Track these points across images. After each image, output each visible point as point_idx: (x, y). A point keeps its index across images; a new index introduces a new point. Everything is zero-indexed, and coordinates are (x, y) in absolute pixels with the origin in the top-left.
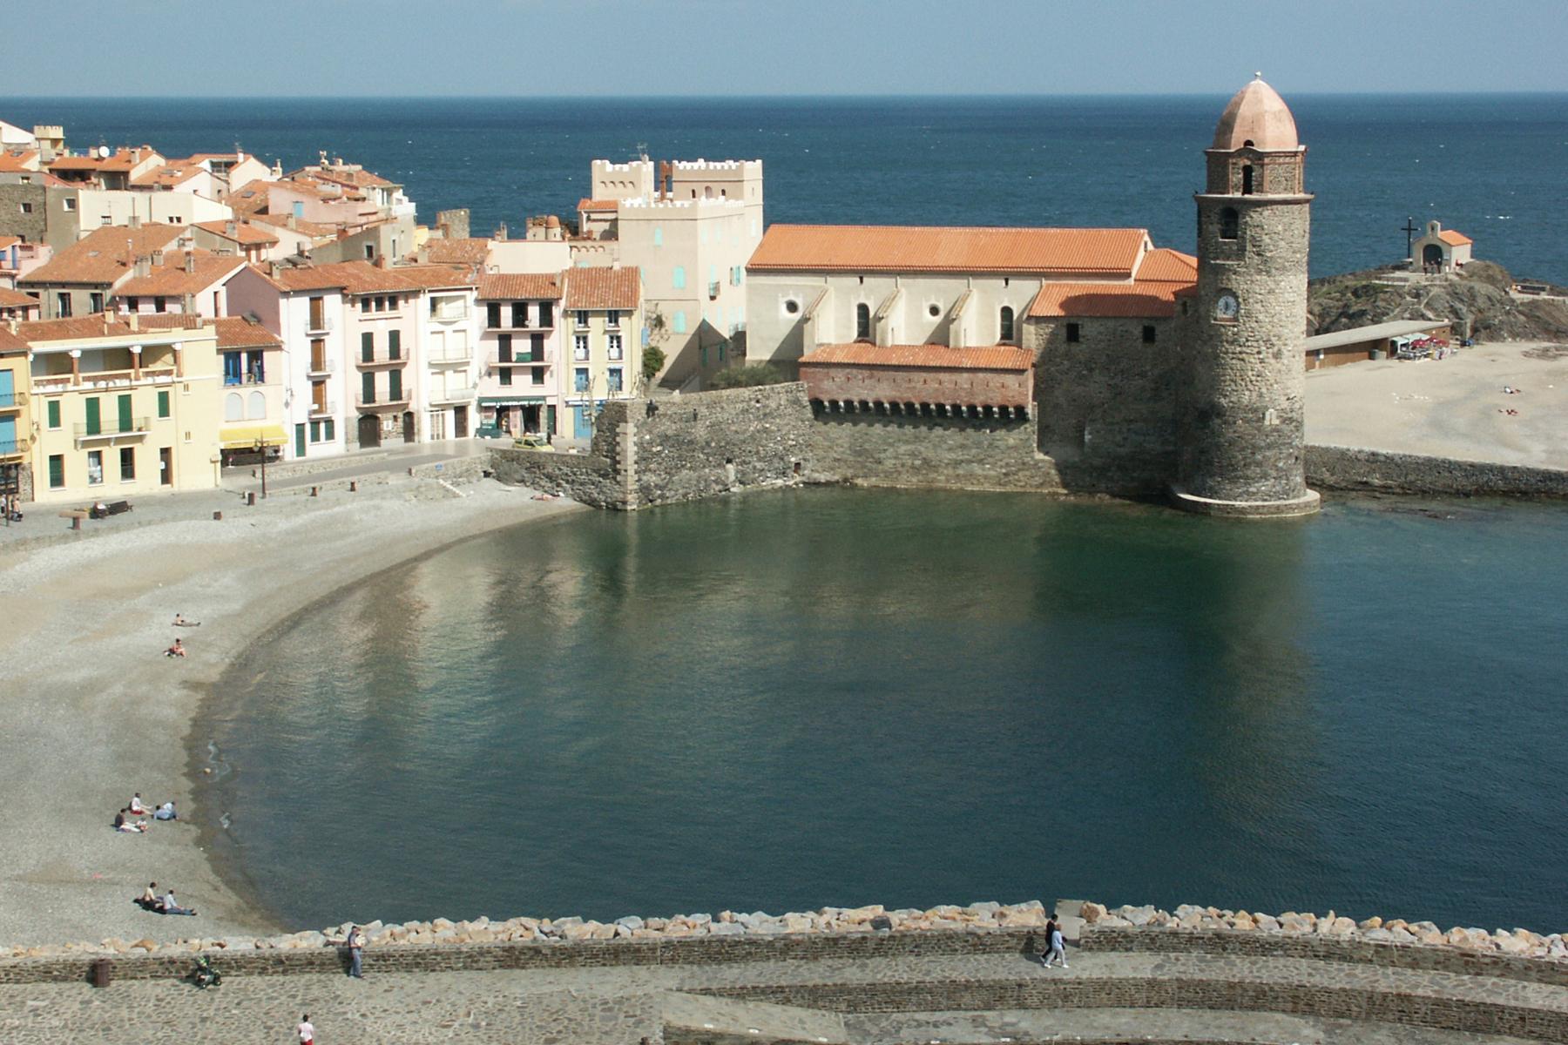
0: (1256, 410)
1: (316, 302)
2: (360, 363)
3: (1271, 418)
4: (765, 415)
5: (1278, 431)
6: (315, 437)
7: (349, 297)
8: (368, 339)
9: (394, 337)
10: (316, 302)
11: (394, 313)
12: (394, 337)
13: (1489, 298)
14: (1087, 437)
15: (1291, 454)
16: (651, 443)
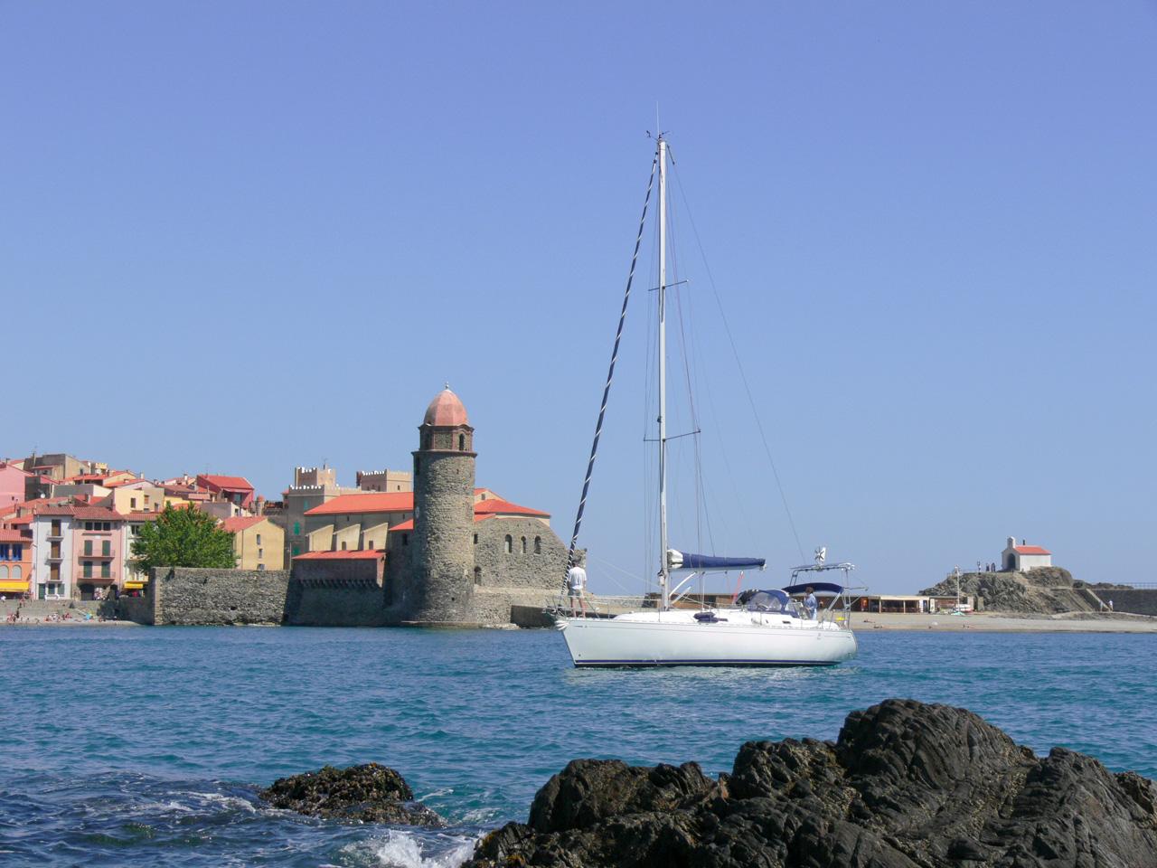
0: (425, 570)
1: (56, 524)
2: (83, 555)
3: (434, 574)
4: (261, 585)
5: (438, 582)
6: (52, 592)
7: (77, 523)
8: (89, 544)
9: (106, 545)
10: (56, 524)
11: (106, 532)
12: (106, 545)
13: (1004, 584)
14: (404, 597)
15: (447, 596)
16: (173, 591)
